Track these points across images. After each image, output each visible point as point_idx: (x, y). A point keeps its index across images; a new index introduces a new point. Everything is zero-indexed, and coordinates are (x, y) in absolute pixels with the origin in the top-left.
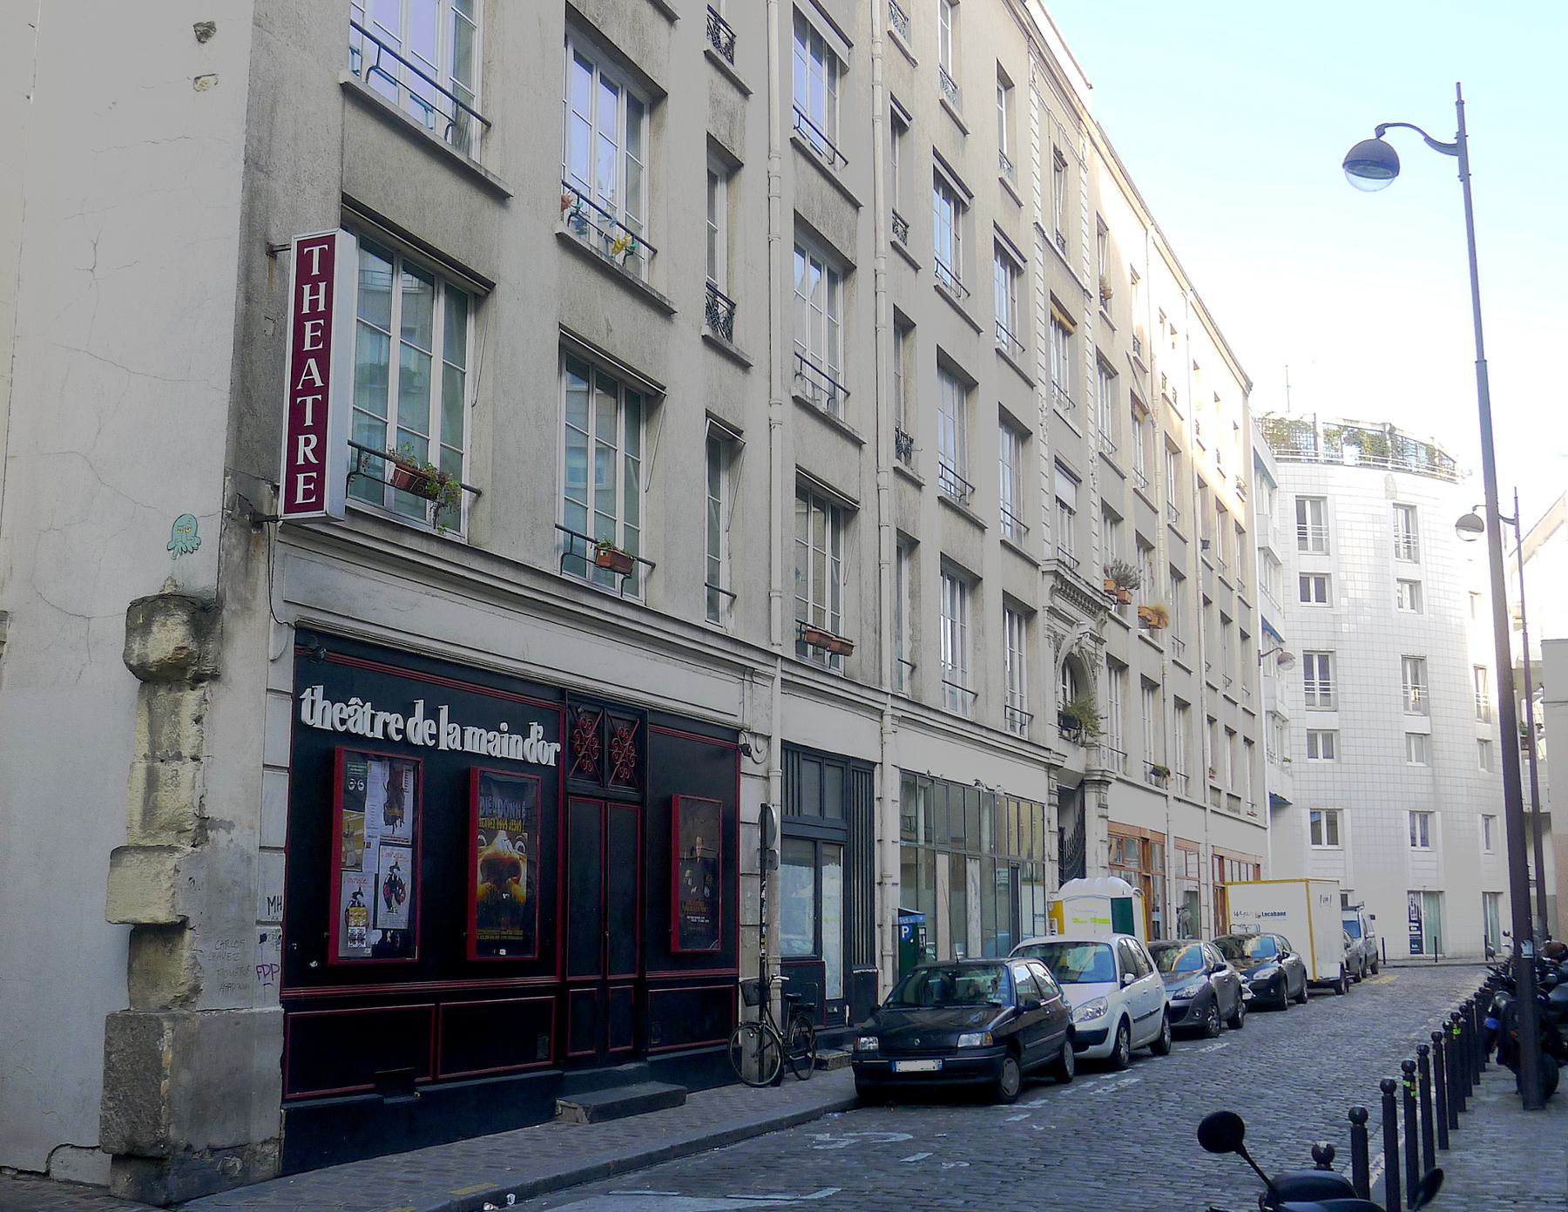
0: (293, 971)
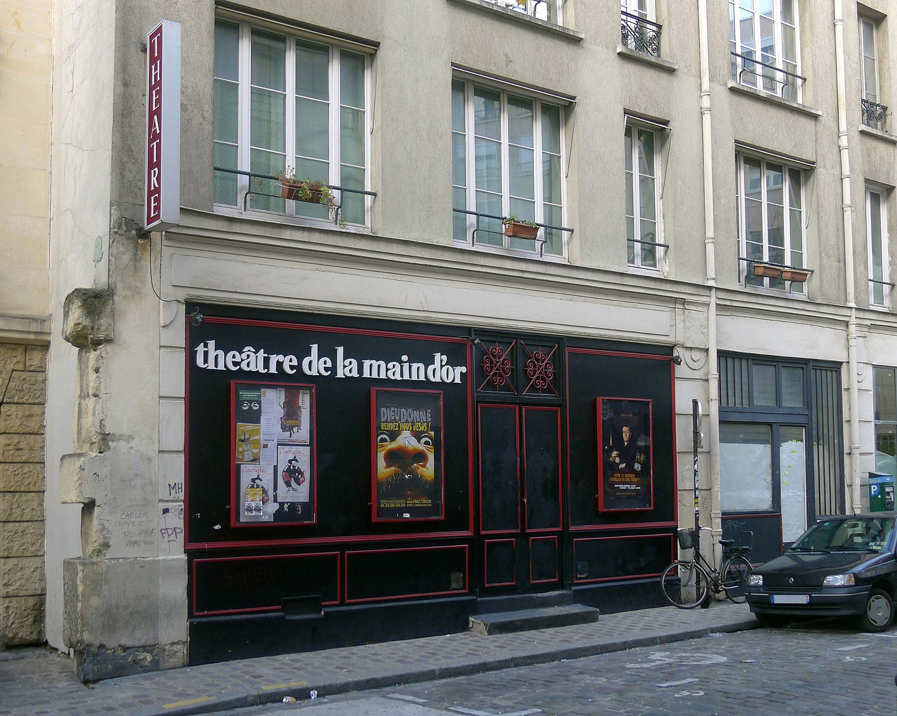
0: (196, 530)
